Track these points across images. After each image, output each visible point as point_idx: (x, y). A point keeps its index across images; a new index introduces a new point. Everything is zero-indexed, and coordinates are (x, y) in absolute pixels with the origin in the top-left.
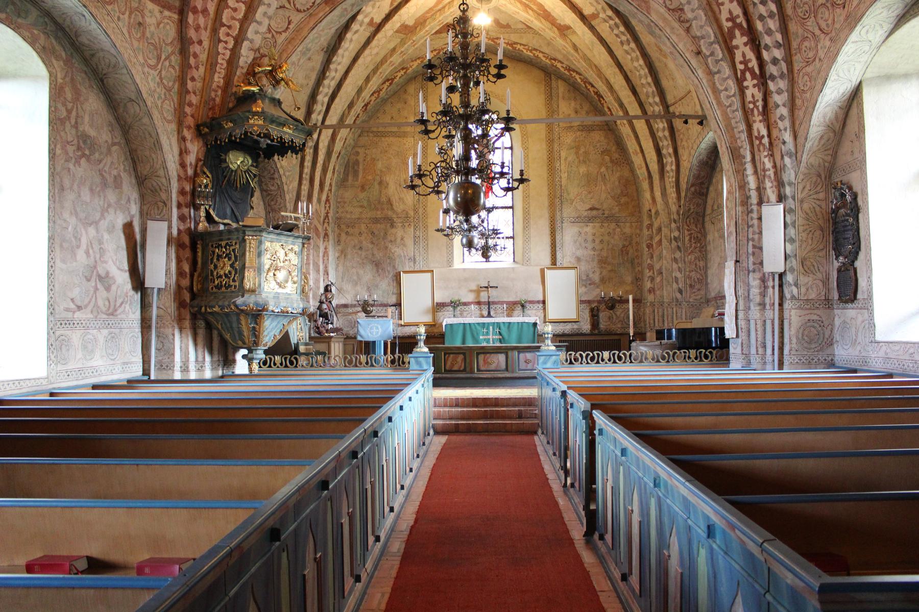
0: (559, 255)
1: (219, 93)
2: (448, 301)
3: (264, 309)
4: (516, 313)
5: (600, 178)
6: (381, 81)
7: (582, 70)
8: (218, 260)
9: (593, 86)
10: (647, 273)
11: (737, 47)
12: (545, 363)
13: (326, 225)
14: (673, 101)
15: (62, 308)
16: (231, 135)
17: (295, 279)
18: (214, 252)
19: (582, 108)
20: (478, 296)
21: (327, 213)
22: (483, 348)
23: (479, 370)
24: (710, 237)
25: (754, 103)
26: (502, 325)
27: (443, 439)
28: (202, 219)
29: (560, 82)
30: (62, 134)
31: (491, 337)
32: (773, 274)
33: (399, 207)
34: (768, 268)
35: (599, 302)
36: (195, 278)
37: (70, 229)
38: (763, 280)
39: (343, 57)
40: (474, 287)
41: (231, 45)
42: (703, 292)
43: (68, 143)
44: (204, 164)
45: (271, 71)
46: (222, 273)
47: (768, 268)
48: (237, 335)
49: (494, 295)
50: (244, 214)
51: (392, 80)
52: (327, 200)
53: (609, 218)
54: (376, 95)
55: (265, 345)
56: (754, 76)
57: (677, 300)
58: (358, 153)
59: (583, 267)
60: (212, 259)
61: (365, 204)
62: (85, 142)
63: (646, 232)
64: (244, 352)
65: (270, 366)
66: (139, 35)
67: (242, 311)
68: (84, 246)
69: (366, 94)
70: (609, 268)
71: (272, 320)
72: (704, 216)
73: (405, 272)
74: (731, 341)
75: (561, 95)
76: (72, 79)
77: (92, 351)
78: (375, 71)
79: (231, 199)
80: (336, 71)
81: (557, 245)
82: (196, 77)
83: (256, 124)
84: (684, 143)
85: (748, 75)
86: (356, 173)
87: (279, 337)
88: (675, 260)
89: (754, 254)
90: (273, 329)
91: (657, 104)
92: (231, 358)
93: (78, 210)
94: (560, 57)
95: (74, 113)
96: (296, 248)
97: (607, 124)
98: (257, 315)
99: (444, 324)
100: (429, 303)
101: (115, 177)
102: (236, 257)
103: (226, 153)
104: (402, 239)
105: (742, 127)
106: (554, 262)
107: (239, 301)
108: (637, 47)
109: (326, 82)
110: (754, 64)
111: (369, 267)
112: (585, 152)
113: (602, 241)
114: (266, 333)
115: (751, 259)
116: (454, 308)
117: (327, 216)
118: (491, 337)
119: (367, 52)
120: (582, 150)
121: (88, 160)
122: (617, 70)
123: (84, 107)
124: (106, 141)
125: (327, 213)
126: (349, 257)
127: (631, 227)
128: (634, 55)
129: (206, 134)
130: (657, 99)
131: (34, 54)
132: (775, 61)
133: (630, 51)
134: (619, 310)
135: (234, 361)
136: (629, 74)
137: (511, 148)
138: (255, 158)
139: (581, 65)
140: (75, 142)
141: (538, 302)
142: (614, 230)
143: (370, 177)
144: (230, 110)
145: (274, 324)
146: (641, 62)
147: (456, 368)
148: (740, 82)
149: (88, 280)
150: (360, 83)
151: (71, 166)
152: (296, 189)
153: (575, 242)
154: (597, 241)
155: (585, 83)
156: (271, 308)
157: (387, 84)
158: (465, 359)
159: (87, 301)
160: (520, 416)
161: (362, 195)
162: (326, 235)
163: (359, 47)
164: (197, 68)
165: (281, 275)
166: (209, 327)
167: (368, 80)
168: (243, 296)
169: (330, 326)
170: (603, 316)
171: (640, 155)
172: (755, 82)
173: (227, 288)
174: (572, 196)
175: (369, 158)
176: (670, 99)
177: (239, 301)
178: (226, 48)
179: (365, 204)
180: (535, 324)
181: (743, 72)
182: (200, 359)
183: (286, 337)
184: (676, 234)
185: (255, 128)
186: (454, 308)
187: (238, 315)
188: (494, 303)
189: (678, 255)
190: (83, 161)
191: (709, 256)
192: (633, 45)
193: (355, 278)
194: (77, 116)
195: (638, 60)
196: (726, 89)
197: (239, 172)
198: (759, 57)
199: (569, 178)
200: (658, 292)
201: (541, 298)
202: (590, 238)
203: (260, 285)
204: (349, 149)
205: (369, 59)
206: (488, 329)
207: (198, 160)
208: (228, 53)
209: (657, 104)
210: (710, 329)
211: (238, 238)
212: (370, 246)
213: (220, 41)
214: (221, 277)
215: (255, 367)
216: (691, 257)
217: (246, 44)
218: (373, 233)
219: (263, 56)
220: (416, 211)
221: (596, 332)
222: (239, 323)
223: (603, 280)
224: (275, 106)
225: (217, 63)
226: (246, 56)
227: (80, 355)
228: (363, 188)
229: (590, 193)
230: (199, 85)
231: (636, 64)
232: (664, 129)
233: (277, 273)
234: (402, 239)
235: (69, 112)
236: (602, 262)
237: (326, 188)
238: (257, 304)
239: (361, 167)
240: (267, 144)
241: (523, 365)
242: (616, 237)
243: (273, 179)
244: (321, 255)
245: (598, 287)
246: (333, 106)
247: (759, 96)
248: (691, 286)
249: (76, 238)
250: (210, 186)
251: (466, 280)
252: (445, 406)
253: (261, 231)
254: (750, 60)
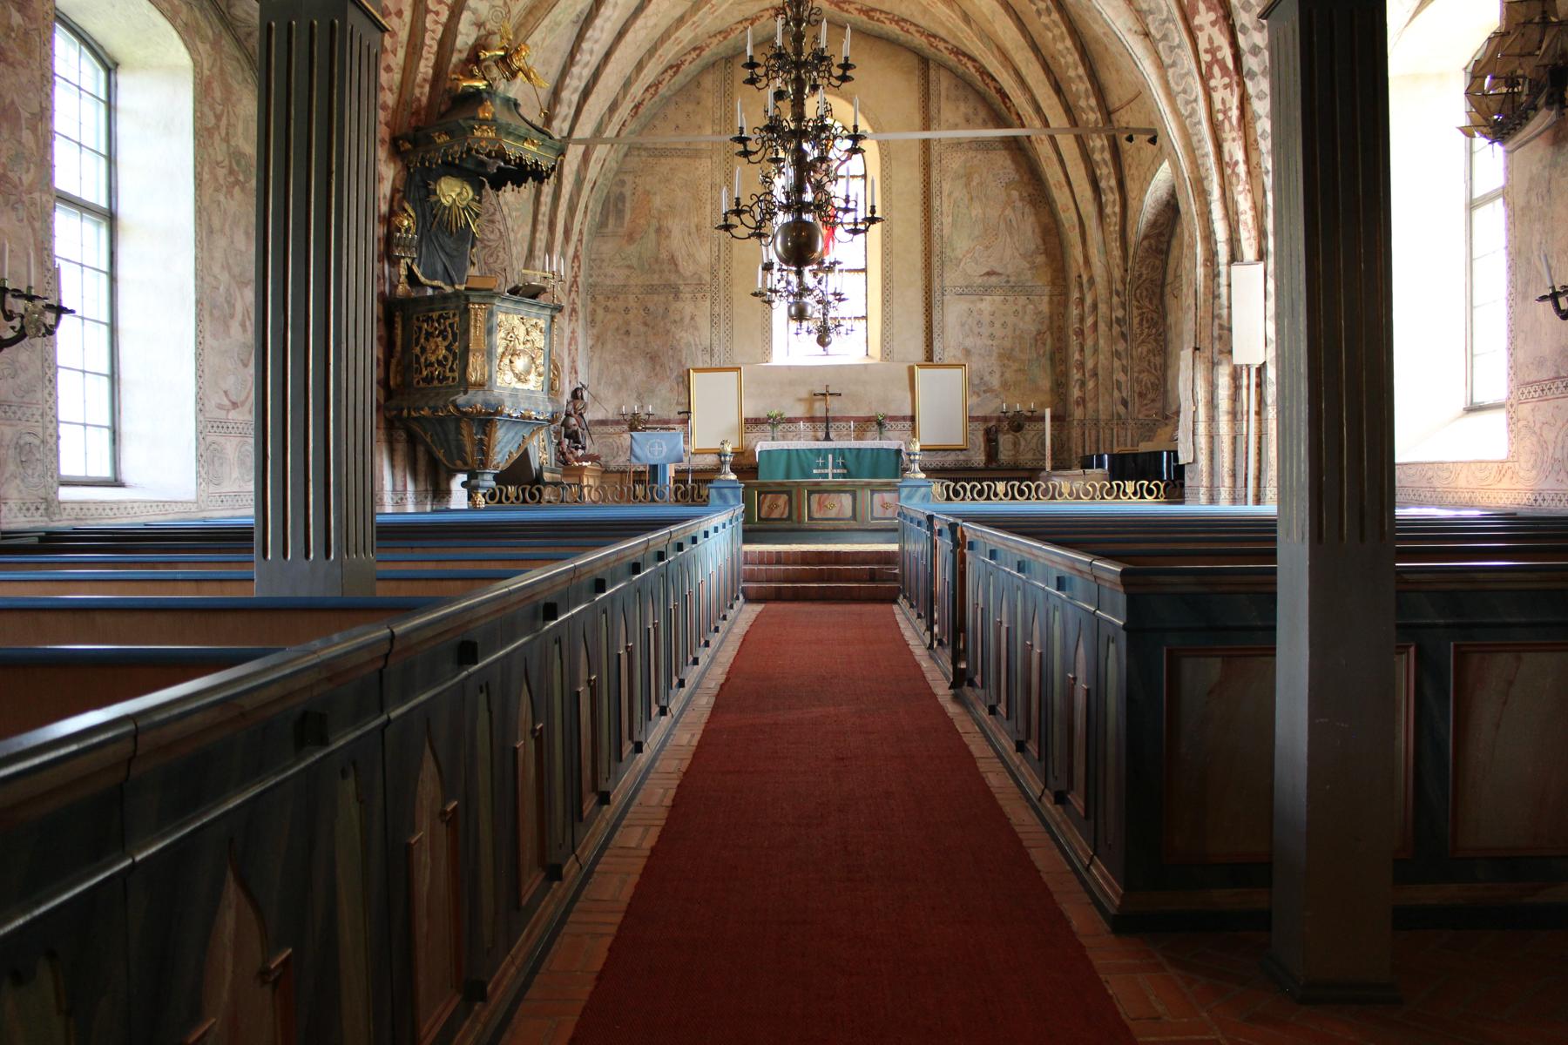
0: (937, 345)
1: (427, 88)
2: (763, 415)
3: (498, 413)
4: (869, 434)
5: (1002, 226)
6: (660, 68)
7: (976, 54)
8: (427, 339)
9: (994, 79)
10: (1076, 375)
11: (1201, 28)
12: (909, 497)
13: (573, 295)
14: (1117, 105)
16: (446, 154)
17: (541, 369)
18: (420, 329)
19: (976, 114)
20: (811, 407)
21: (576, 277)
22: (817, 484)
23: (810, 518)
24: (1171, 319)
25: (1225, 113)
26: (847, 454)
27: (758, 608)
28: (403, 279)
29: (942, 72)
30: (211, 150)
31: (829, 471)
32: (1249, 367)
33: (687, 268)
34: (1238, 359)
35: (999, 419)
36: (393, 368)
38: (1236, 375)
39: (602, 30)
40: (804, 394)
41: (444, 18)
42: (1159, 405)
44: (404, 197)
45: (503, 58)
46: (433, 359)
47: (1238, 359)
48: (455, 451)
49: (836, 407)
50: (462, 270)
51: (678, 66)
52: (576, 256)
53: (1014, 288)
54: (652, 90)
55: (496, 467)
56: (1225, 71)
57: (1119, 417)
58: (623, 183)
59: (976, 364)
60: (418, 339)
61: (634, 262)
62: (238, 163)
63: (1074, 311)
64: (462, 477)
65: (500, 501)
67: (465, 414)
68: (239, 316)
69: (637, 90)
70: (1015, 366)
71: (508, 430)
72: (1163, 285)
73: (696, 370)
74: (1187, 469)
75: (943, 93)
76: (222, 70)
78: (652, 52)
79: (442, 248)
80: (591, 52)
81: (935, 330)
82: (393, 66)
83: (484, 136)
84: (1133, 171)
85: (1216, 70)
86: (620, 214)
87: (516, 456)
88: (1117, 354)
89: (1220, 337)
90: (508, 442)
91: (1092, 109)
92: (443, 486)
94: (942, 33)
95: (224, 121)
96: (542, 324)
97: (1015, 139)
98: (487, 420)
99: (758, 450)
100: (733, 420)
102: (454, 334)
103: (436, 180)
104: (692, 318)
105: (1209, 147)
106: (929, 358)
107: (461, 399)
108: (1062, 17)
109: (575, 70)
110: (1226, 53)
111: (640, 362)
112: (981, 184)
113: (1004, 325)
114: (497, 449)
115: (1217, 346)
116: (774, 426)
117: (575, 281)
118: (829, 471)
119: (640, 22)
120: (976, 180)
121: (243, 189)
122: (1031, 55)
125: (576, 277)
126: (609, 346)
127: (1051, 302)
128: (1057, 32)
129: (407, 151)
130: (1093, 102)
131: (175, 34)
132: (1255, 50)
133: (1051, 25)
134: (1030, 430)
135: (448, 492)
136: (1049, 61)
137: (865, 176)
138: (478, 188)
139: (976, 47)
140: (226, 163)
141: (904, 418)
142: (1024, 307)
143: (642, 221)
144: (442, 116)
145: (511, 434)
146: (1069, 43)
147: (776, 515)
148: (1205, 79)
149: (246, 366)
150: (628, 71)
151: (222, 198)
152: (528, 238)
153: (963, 325)
154: (998, 325)
155: (982, 74)
156: (506, 411)
157: (671, 72)
158: (790, 500)
159: (243, 398)
160: (872, 576)
161: (632, 249)
162: (574, 310)
163: (627, 15)
164: (394, 53)
165: (520, 363)
166: (412, 440)
167: (640, 66)
168: (466, 392)
169: (580, 452)
170: (1005, 441)
171: (1066, 189)
172: (1227, 80)
173: (440, 381)
174: (959, 253)
175: (640, 189)
176: (1114, 100)
177: (461, 399)
178: (437, 22)
179: (634, 262)
180: (899, 452)
181: (1209, 66)
182: (399, 487)
183: (525, 456)
184: (1120, 313)
185: (484, 144)
186: (774, 426)
187: (458, 420)
188: (835, 419)
189: (1121, 346)
190: (237, 189)
191: (1170, 348)
192: (1056, 16)
193: (619, 379)
194: (229, 125)
195: (1063, 40)
196: (1185, 91)
197: (454, 209)
198: (1234, 44)
199: (954, 224)
200: (1090, 405)
201: (908, 413)
202: (986, 319)
203: (490, 376)
204: (611, 175)
205: (642, 34)
206: (826, 458)
207: (394, 191)
208: (440, 29)
209: (1092, 109)
210: (1161, 453)
211: (457, 307)
212: (643, 329)
213: (427, 11)
214: (431, 364)
215: (481, 501)
216: (1143, 349)
217: (466, 17)
218: (646, 309)
219: (491, 33)
220: (714, 273)
221: (994, 465)
222: (458, 431)
223: (1005, 385)
224: (509, 109)
225: (423, 44)
226: (466, 35)
228: (631, 238)
229: (987, 248)
230: (397, 77)
231: (1060, 46)
232: (1102, 149)
233: (515, 359)
234: (692, 318)
235: (218, 118)
236: (1006, 356)
237: (574, 237)
238: (486, 404)
239: (628, 205)
240: (499, 168)
241: (878, 512)
242: (1027, 318)
243: (493, 222)
244: (566, 342)
245: (997, 396)
246: (586, 108)
247: (1234, 102)
248: (1141, 395)
250: (413, 230)
251: (792, 383)
252: (761, 563)
253: (492, 297)
254: (1219, 48)
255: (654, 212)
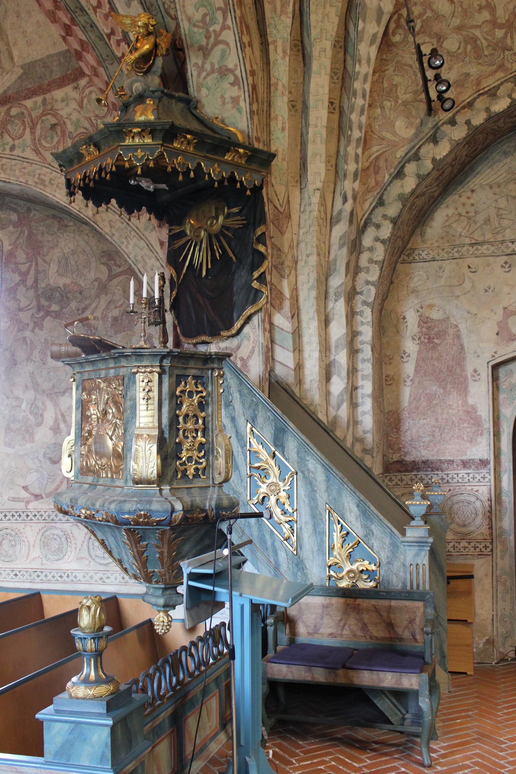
15: (5, 498)
37: (24, 406)
43: (20, 310)
62: (50, 298)
66: (56, 140)
77: (60, 550)
93: (40, 380)
101: (115, 319)
121: (57, 315)
123: (47, 258)
124: (96, 280)
194: (37, 272)
227: (36, 552)
249: (35, 415)
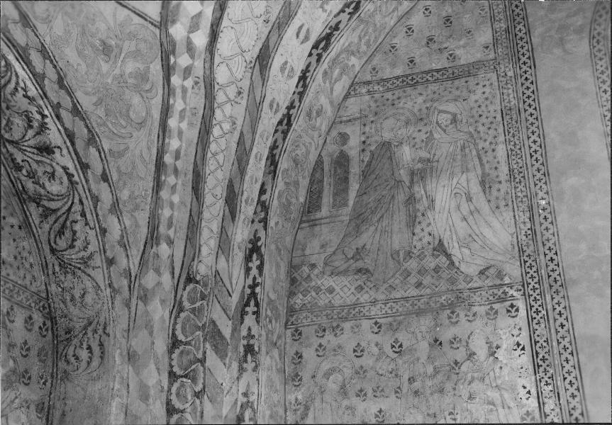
13: (249, 320)
58: (344, 138)
162: (249, 349)
255: (404, 175)
